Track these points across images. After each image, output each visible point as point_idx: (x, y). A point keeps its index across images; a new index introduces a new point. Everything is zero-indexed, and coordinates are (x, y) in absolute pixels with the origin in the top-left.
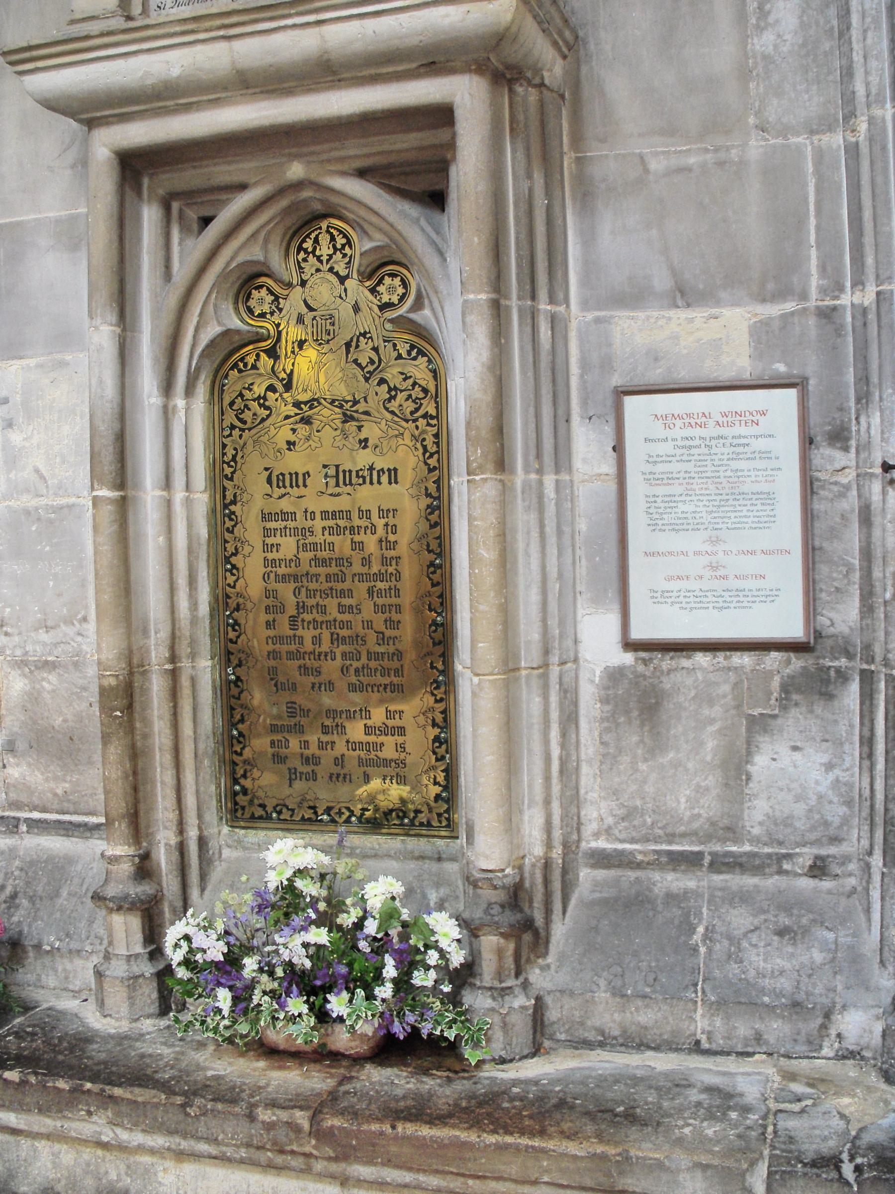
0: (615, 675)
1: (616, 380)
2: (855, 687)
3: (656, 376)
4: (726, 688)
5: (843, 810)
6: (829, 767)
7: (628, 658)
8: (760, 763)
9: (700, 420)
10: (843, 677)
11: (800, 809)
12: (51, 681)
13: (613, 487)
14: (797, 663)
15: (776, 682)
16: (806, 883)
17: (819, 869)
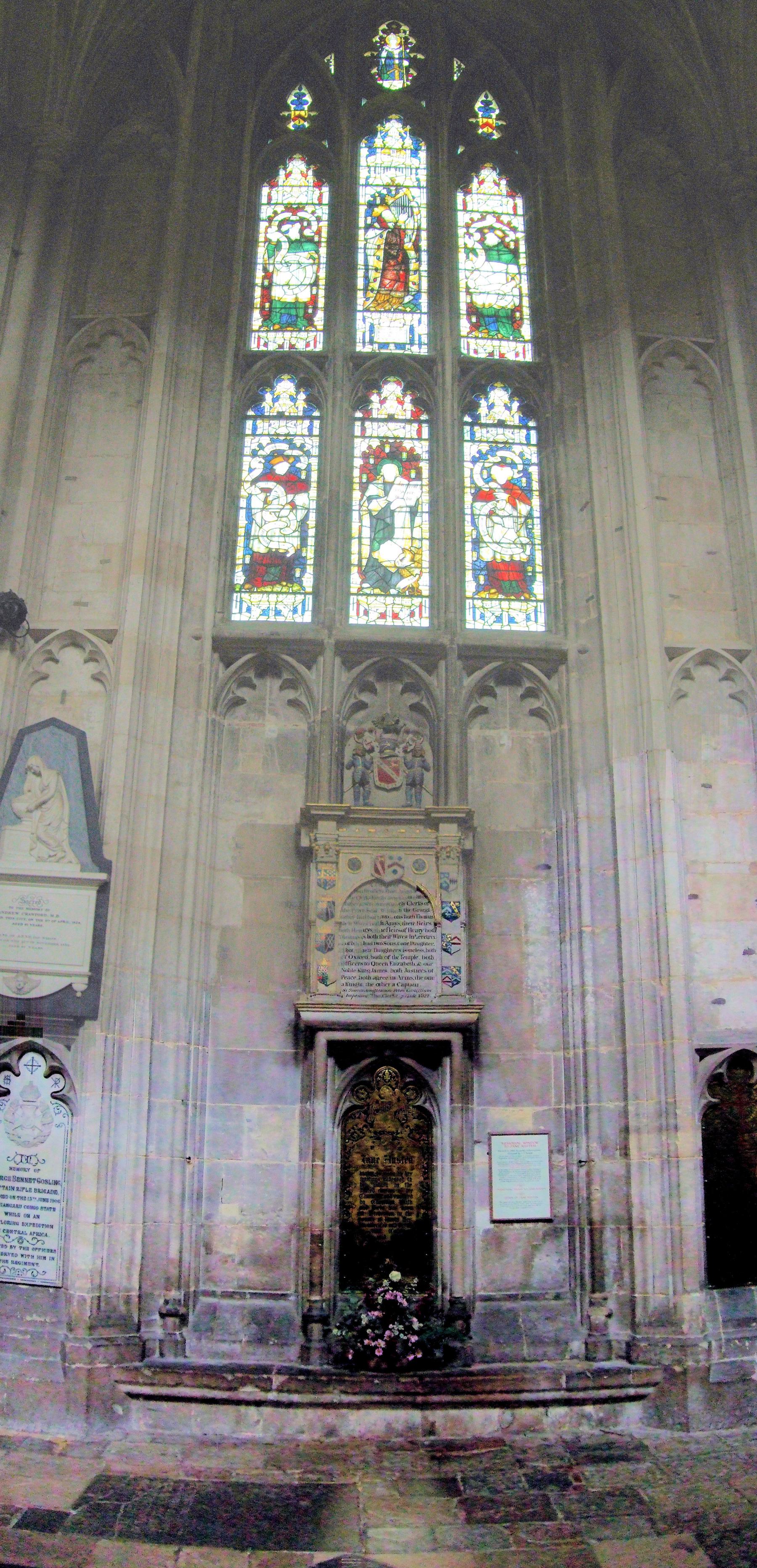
0: (487, 1232)
1: (489, 1130)
2: (566, 1233)
3: (501, 1130)
4: (524, 1236)
5: (563, 1277)
6: (559, 1261)
7: (492, 1226)
8: (537, 1261)
9: (516, 1145)
10: (562, 1230)
11: (550, 1277)
12: (263, 1235)
13: (487, 1166)
14: (548, 1226)
15: (541, 1233)
16: (553, 1302)
17: (557, 1297)
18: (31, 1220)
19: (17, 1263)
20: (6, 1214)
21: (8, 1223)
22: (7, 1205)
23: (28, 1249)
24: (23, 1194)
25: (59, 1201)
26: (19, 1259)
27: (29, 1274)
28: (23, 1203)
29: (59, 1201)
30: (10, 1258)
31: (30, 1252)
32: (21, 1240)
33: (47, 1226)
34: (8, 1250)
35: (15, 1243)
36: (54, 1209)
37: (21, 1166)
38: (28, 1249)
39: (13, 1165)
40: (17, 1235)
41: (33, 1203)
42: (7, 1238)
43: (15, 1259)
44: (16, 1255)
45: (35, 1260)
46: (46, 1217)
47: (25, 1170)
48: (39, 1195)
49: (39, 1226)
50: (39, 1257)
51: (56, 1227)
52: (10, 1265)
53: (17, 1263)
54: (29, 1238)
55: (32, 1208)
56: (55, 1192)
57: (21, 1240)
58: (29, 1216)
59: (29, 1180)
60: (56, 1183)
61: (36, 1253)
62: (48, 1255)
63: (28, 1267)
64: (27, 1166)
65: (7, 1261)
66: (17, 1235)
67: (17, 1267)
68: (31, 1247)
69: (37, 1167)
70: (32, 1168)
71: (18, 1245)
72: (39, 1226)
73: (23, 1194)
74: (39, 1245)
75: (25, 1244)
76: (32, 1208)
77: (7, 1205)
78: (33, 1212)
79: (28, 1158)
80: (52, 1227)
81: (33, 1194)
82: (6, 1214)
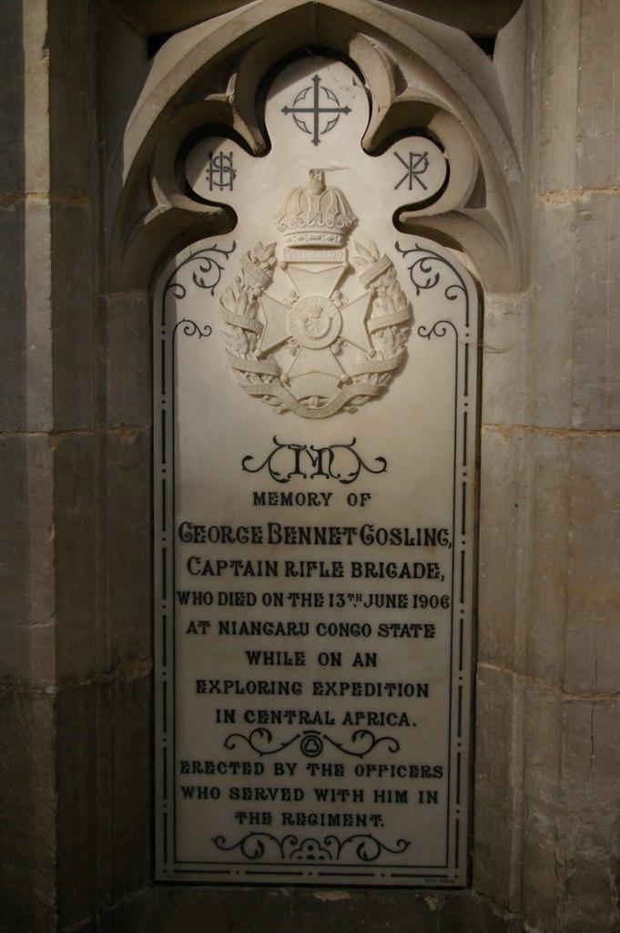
18: (348, 673)
19: (302, 819)
20: (253, 657)
21: (263, 688)
22: (257, 628)
23: (339, 770)
24: (314, 584)
25: (444, 602)
26: (310, 805)
27: (349, 854)
28: (313, 616)
29: (444, 602)
30: (276, 807)
31: (350, 781)
32: (311, 744)
33: (404, 690)
34: (269, 780)
35: (293, 754)
36: (430, 631)
37: (298, 485)
38: (339, 770)
39: (265, 483)
40: (297, 728)
41: (351, 614)
42: (260, 742)
43: (294, 807)
44: (299, 795)
45: (368, 807)
46: (398, 660)
47: (312, 499)
48: (366, 586)
49: (373, 689)
50: (379, 796)
51: (439, 692)
52: (278, 829)
53: (302, 819)
54: (340, 733)
55: (346, 630)
56: (431, 571)
57: (311, 744)
58: (336, 660)
59: (330, 536)
60: (432, 537)
61: (369, 784)
62: (413, 786)
63: (342, 832)
64: (319, 485)
65: (267, 818)
66: (297, 728)
67: (303, 832)
68: (350, 763)
69: (357, 488)
70: (341, 492)
71: (303, 761)
72: (373, 689)
73: (314, 584)
74: (380, 755)
75: (329, 755)
76: (346, 630)
77: (257, 628)
78: (349, 647)
79: (323, 458)
80: (423, 690)
81: (348, 584)
82: (253, 657)
